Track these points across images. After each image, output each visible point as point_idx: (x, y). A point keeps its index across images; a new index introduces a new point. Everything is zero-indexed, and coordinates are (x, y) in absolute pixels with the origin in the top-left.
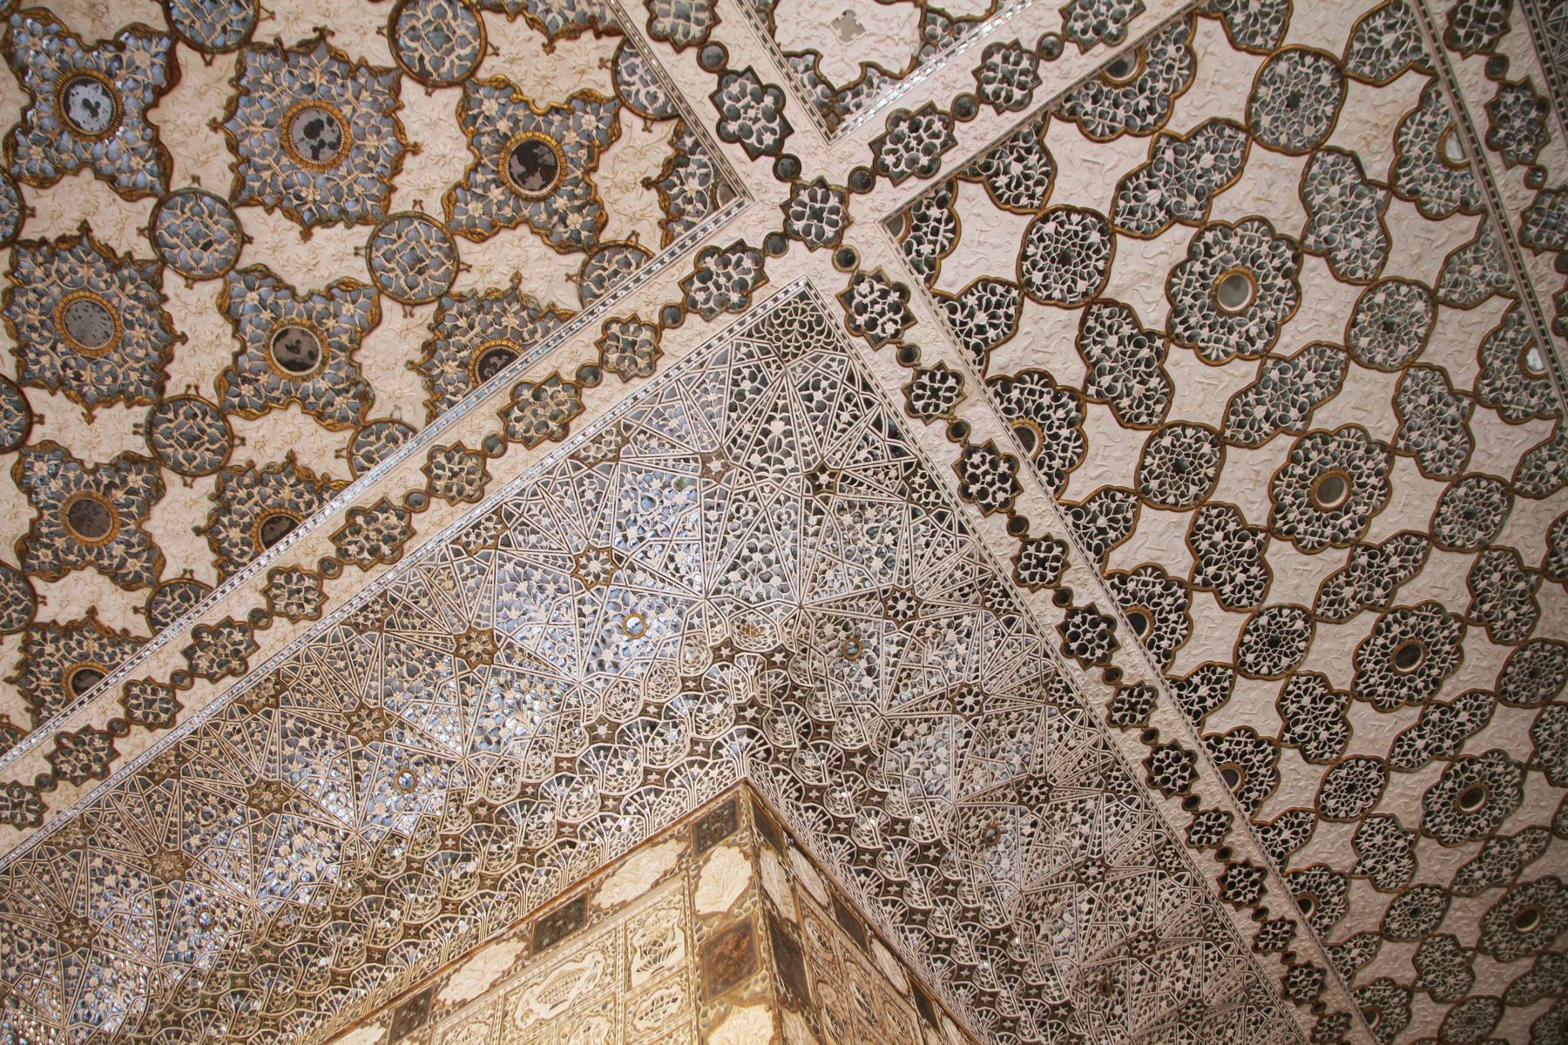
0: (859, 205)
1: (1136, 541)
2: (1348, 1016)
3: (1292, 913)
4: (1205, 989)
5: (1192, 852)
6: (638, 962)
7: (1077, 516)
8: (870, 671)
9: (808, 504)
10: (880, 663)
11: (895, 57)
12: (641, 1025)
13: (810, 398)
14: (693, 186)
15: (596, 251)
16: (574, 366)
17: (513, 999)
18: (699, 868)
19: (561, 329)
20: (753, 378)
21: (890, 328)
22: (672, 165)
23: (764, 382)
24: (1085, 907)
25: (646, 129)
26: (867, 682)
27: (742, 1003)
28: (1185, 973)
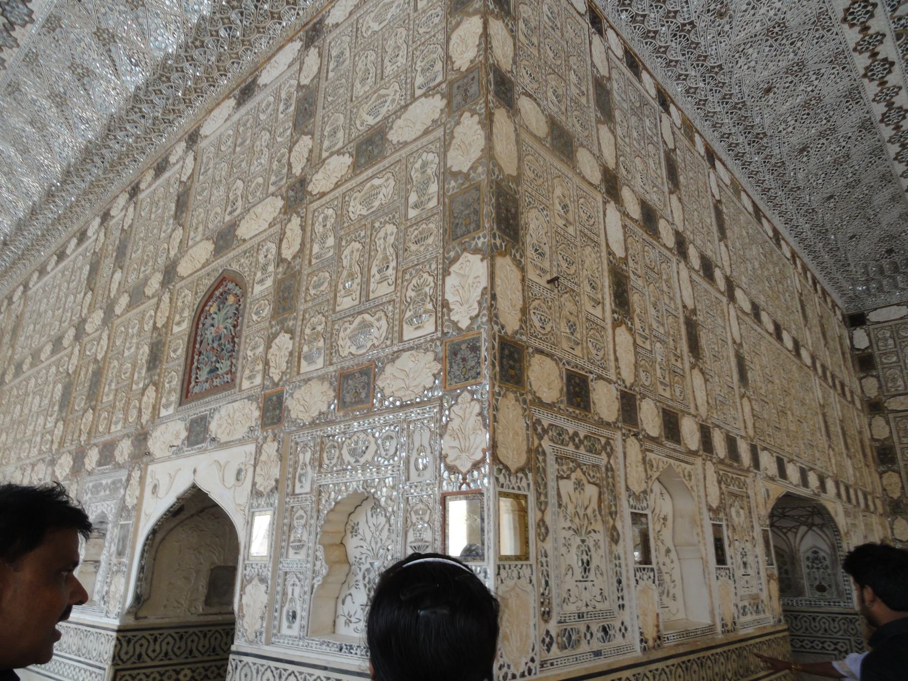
2: (884, 35)
4: (788, 16)
17: (361, 21)
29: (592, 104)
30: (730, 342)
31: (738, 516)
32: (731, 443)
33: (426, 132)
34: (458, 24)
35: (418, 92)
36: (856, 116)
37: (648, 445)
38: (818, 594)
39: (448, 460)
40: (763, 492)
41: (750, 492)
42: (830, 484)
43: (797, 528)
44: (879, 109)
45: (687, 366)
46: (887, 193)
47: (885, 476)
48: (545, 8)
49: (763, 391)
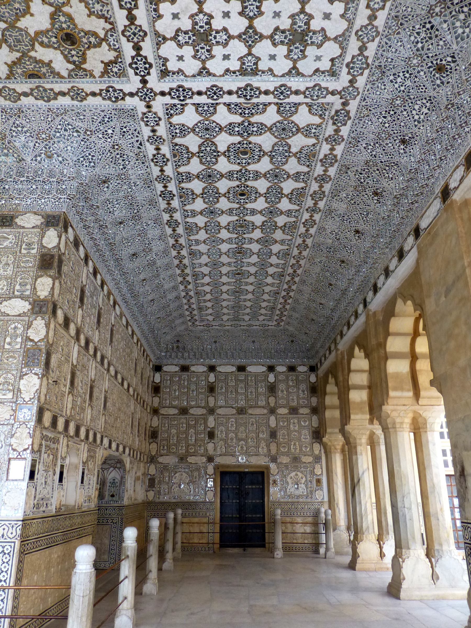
0: (159, 98)
1: (190, 184)
3: (186, 255)
4: (158, 261)
5: (169, 238)
6: (24, 246)
7: (178, 174)
8: (107, 187)
9: (109, 151)
10: (111, 186)
11: (189, 72)
12: (22, 264)
13: (122, 129)
14: (115, 70)
15: (79, 69)
16: (59, 90)
18: (46, 231)
19: (59, 80)
20: (109, 118)
21: (152, 124)
22: (111, 62)
23: (111, 120)
24: (137, 240)
25: (109, 50)
26: (105, 189)
27: (47, 276)
28: (155, 257)
29: (78, 301)
30: (103, 391)
31: (91, 466)
32: (95, 435)
33: (19, 315)
34: (41, 276)
35: (16, 293)
36: (174, 294)
37: (70, 439)
38: (111, 498)
39: (13, 447)
40: (101, 454)
41: (97, 455)
42: (127, 450)
43: (109, 468)
44: (183, 294)
45: (87, 405)
46: (181, 320)
47: (152, 444)
48: (71, 263)
49: (111, 411)
